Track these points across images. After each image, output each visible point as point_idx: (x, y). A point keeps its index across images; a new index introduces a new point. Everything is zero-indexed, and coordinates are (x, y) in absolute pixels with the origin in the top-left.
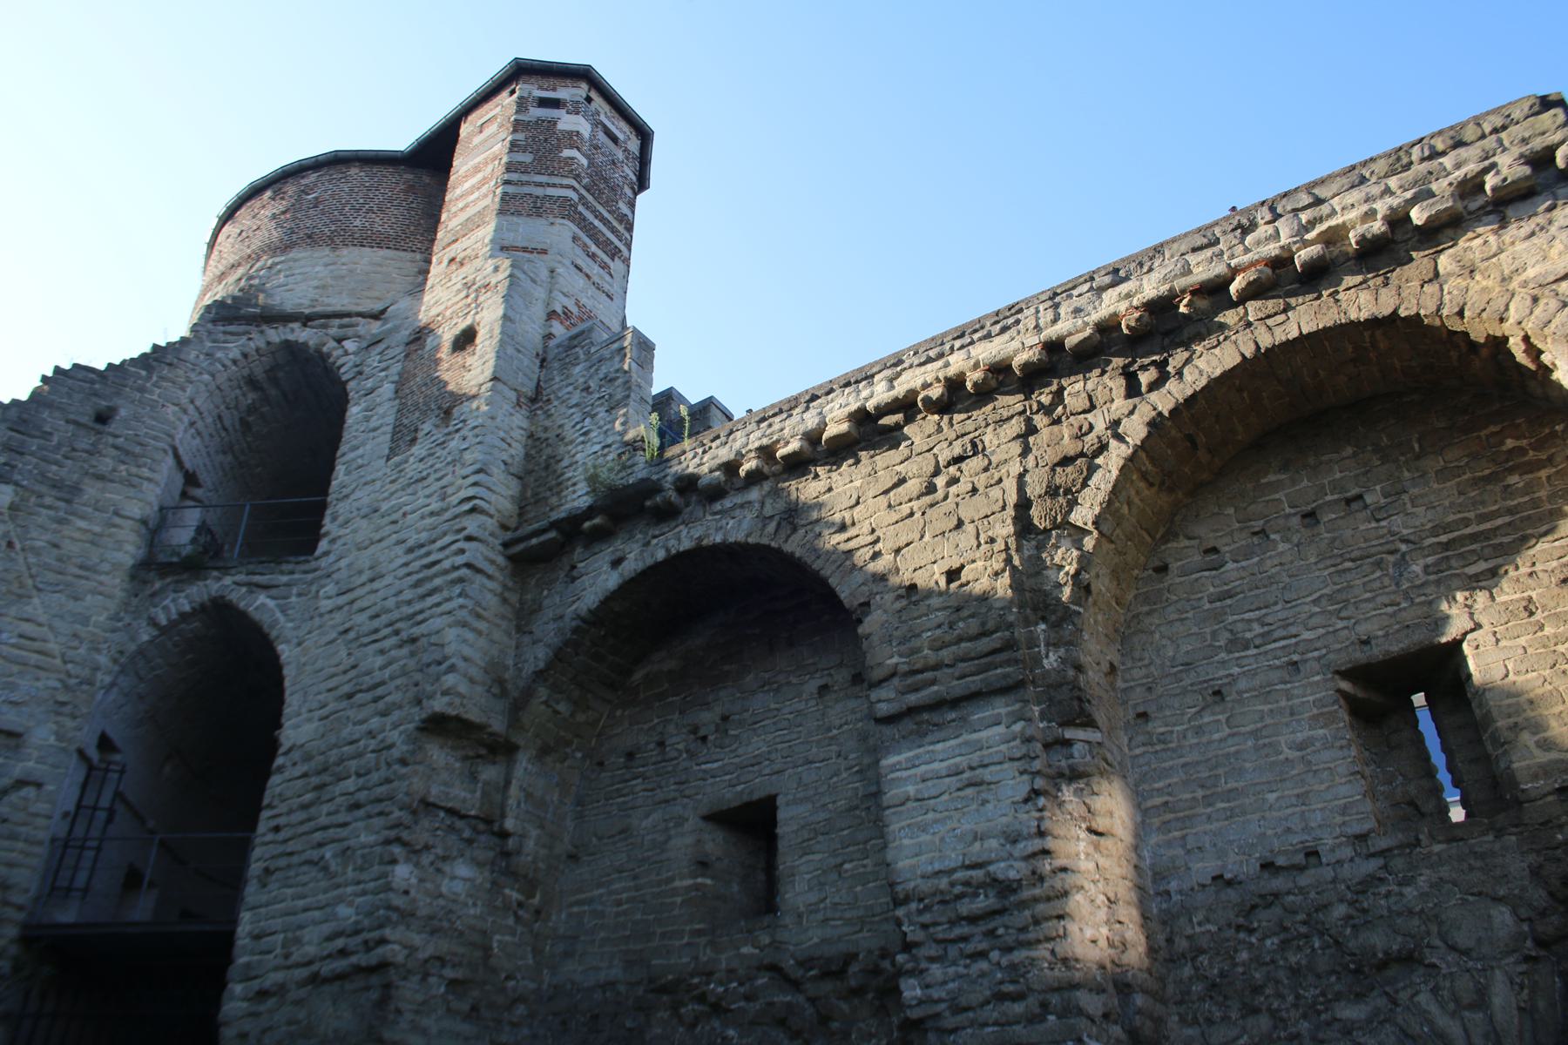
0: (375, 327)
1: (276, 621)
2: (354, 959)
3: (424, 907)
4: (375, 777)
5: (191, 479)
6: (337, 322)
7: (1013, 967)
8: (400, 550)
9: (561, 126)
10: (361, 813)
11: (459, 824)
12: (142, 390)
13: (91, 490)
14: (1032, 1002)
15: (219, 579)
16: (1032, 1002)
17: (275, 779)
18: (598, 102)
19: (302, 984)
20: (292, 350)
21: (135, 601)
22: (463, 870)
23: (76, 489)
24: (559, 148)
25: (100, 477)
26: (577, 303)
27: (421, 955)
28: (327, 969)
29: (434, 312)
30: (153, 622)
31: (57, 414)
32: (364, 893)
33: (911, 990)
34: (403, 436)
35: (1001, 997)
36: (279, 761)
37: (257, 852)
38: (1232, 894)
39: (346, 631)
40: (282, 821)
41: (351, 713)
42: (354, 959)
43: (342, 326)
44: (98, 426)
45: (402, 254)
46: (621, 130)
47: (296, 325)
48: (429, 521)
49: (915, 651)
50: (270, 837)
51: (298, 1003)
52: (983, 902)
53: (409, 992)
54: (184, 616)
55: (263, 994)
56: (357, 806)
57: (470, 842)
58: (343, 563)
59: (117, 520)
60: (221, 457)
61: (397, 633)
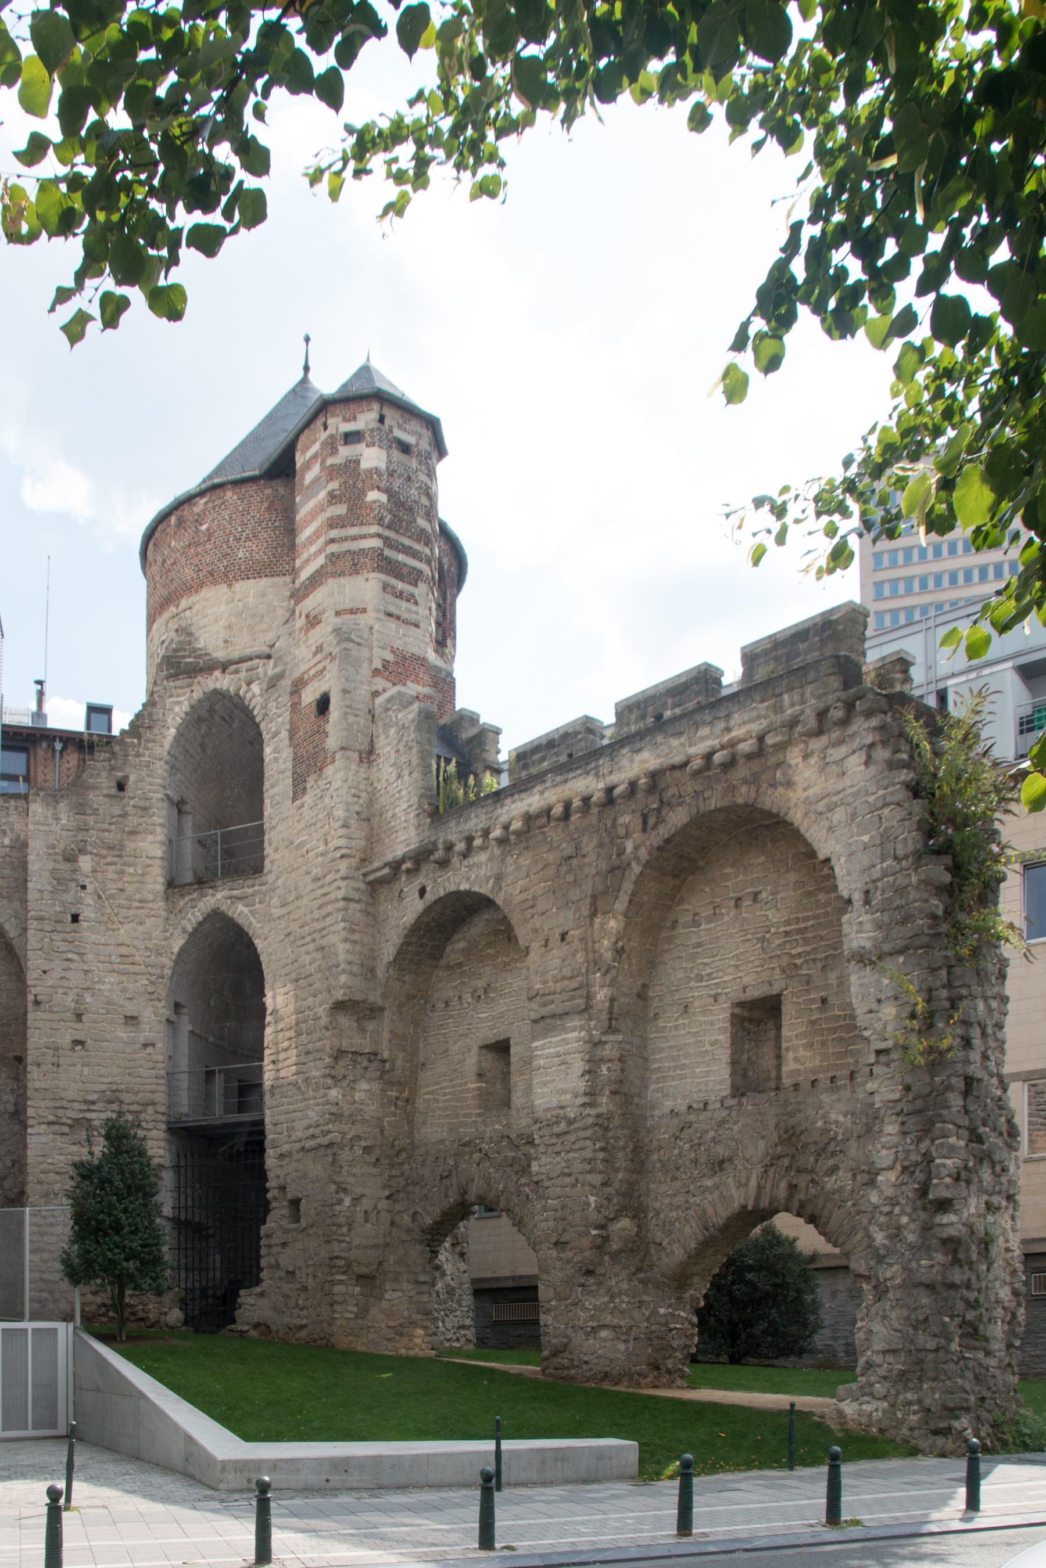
0: (271, 669)
1: (251, 923)
2: (318, 1140)
3: (347, 1110)
4: (315, 1036)
6: (244, 666)
7: (568, 1161)
9: (365, 465)
10: (311, 1057)
11: (359, 1059)
15: (213, 895)
17: (268, 1031)
19: (298, 1152)
20: (218, 695)
21: (172, 917)
22: (364, 1085)
24: (363, 493)
26: (393, 652)
27: (348, 1136)
29: (303, 668)
30: (184, 931)
39: (288, 935)
42: (318, 1140)
43: (247, 671)
45: (277, 580)
47: (217, 673)
48: (320, 859)
49: (546, 982)
50: (271, 1067)
51: (298, 1161)
52: (563, 1126)
53: (345, 1155)
54: (200, 924)
55: (282, 1156)
56: (308, 1053)
57: (366, 1068)
58: (280, 882)
61: (314, 940)
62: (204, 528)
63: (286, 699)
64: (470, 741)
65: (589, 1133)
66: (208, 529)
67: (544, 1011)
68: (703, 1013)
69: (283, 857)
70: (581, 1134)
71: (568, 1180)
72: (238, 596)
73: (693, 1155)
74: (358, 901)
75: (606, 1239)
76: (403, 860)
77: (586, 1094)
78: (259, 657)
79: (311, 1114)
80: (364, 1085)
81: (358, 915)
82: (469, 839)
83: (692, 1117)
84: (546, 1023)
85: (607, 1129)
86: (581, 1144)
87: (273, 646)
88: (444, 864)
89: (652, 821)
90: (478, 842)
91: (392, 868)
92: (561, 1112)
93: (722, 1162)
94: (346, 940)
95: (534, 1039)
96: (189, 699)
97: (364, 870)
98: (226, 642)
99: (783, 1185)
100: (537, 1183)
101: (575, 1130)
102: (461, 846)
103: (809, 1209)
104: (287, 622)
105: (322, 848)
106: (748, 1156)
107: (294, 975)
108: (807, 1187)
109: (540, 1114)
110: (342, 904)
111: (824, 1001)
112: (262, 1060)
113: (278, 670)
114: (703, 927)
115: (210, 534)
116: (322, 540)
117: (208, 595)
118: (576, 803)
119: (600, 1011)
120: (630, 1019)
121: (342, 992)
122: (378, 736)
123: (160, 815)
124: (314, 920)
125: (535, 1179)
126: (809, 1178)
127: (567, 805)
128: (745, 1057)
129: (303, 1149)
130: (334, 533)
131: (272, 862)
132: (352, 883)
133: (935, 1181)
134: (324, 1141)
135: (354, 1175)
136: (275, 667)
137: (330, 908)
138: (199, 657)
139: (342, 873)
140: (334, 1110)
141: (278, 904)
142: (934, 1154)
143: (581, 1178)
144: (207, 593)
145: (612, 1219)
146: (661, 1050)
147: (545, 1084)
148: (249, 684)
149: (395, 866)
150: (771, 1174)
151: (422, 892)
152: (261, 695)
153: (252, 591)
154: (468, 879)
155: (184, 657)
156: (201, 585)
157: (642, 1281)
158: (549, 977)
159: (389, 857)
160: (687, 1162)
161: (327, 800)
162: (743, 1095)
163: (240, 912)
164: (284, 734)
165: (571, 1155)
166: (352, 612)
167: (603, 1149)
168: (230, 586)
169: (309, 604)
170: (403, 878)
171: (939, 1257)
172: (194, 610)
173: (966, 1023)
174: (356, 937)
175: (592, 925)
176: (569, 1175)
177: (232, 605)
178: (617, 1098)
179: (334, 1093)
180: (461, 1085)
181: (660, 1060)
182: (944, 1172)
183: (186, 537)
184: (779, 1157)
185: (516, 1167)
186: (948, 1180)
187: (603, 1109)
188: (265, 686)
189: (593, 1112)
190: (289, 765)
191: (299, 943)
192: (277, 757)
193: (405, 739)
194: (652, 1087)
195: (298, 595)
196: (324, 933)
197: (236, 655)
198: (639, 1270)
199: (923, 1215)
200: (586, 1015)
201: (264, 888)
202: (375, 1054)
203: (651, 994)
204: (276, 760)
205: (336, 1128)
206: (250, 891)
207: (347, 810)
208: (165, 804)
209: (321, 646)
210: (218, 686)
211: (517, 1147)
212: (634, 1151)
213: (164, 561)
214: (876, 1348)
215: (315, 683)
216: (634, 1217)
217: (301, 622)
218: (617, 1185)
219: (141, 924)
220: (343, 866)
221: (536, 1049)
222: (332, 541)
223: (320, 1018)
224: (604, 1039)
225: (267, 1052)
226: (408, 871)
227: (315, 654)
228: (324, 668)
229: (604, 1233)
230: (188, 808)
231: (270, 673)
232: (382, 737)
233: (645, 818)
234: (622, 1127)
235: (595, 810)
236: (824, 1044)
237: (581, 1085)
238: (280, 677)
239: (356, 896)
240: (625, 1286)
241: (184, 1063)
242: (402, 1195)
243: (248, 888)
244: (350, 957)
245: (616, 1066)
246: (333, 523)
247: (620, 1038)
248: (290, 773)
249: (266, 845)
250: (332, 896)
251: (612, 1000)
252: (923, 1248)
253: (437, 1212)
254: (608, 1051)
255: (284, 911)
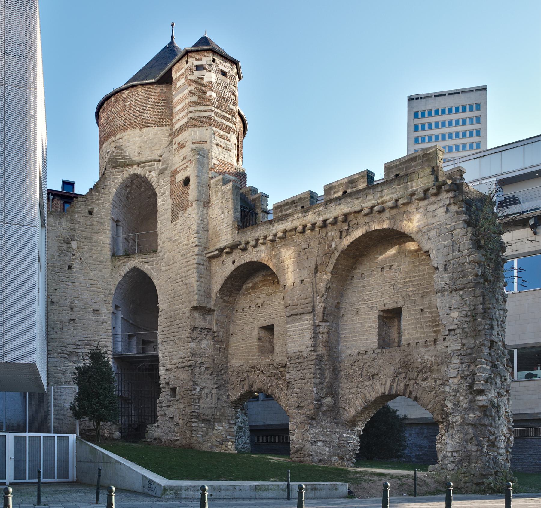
0: (160, 166)
1: (151, 273)
2: (185, 364)
4: (183, 321)
5: (117, 222)
7: (304, 373)
8: (180, 255)
10: (181, 329)
11: (203, 331)
12: (98, 200)
13: (95, 238)
14: (306, 381)
15: (134, 261)
16: (306, 381)
17: (160, 318)
18: (218, 60)
20: (136, 176)
21: (114, 269)
23: (91, 238)
25: (96, 233)
26: (218, 160)
28: (180, 365)
29: (177, 166)
30: (120, 275)
31: (79, 215)
32: (184, 349)
33: (288, 376)
34: (175, 216)
35: (302, 379)
36: (160, 313)
37: (159, 337)
38: (352, 358)
40: (163, 329)
41: (175, 302)
42: (185, 364)
44: (91, 216)
45: (163, 128)
46: (227, 67)
47: (135, 167)
48: (185, 247)
49: (293, 300)
50: (162, 333)
51: (174, 372)
52: (301, 359)
53: (197, 370)
54: (128, 272)
57: (206, 335)
58: (165, 256)
59: (104, 245)
60: (123, 210)
62: (128, 104)
63: (168, 179)
64: (254, 200)
65: (313, 362)
66: (130, 104)
67: (292, 312)
68: (365, 314)
69: (167, 246)
70: (309, 363)
71: (303, 381)
72: (145, 134)
73: (360, 372)
74: (203, 265)
75: (321, 405)
76: (225, 248)
77: (312, 346)
78: (154, 161)
79: (181, 353)
80: (205, 342)
81: (203, 270)
82: (257, 240)
83: (360, 357)
84: (293, 316)
85: (321, 361)
86: (310, 366)
87: (161, 156)
88: (244, 250)
89: (344, 234)
90: (261, 241)
91: (219, 251)
92: (301, 353)
93: (373, 375)
94: (198, 281)
95: (287, 324)
96: (122, 177)
97: (206, 252)
98: (139, 153)
99: (402, 385)
100: (289, 382)
101: (307, 361)
102: (253, 243)
103: (414, 394)
104: (168, 146)
105: (186, 242)
106: (386, 373)
107: (172, 295)
108: (413, 386)
109: (290, 355)
110: (196, 265)
111: (422, 310)
112: (157, 330)
113: (164, 166)
114: (365, 279)
115: (131, 106)
116: (186, 111)
117: (130, 133)
118: (309, 226)
119: (319, 313)
120: (332, 315)
121: (196, 302)
122: (213, 196)
123: (109, 226)
124: (182, 272)
125: (288, 381)
126: (414, 381)
127: (305, 227)
128: (384, 333)
129: (177, 367)
130: (191, 109)
131: (161, 248)
132: (200, 257)
133: (477, 382)
134: (189, 364)
135: (201, 378)
136: (162, 165)
137: (190, 267)
138: (126, 159)
139: (196, 253)
140: (192, 351)
141: (165, 265)
142: (477, 371)
143: (310, 380)
144: (130, 132)
145: (323, 398)
146: (345, 329)
147: (293, 342)
148: (150, 172)
149: (221, 250)
150: (397, 379)
151: (234, 262)
152: (156, 177)
153: (150, 132)
154: (256, 257)
155: (120, 159)
156: (127, 128)
157: (336, 423)
158: (295, 298)
159: (218, 247)
160: (357, 375)
161: (189, 222)
162: (383, 348)
163: (146, 268)
164: (167, 194)
165: (305, 371)
166: (200, 143)
167: (319, 369)
168: (141, 129)
169: (179, 138)
170: (224, 256)
171: (478, 413)
172: (124, 139)
173: (492, 319)
174: (202, 280)
175: (315, 277)
176: (304, 379)
177: (141, 138)
178: (326, 348)
179: (192, 344)
180: (250, 343)
181: (345, 334)
182: (481, 379)
183: (120, 107)
184: (400, 373)
185: (276, 377)
186: (482, 382)
187: (320, 353)
188: (157, 173)
189: (316, 354)
190: (170, 207)
191: (175, 282)
192: (164, 204)
193: (225, 197)
194: (341, 344)
195: (174, 135)
196: (187, 278)
197: (144, 159)
198: (335, 418)
199: (470, 396)
200: (312, 314)
201: (157, 258)
202: (211, 329)
203: (341, 307)
204: (163, 204)
205: (193, 359)
206: (151, 259)
207: (198, 226)
208: (111, 221)
209: (186, 157)
210: (136, 172)
211: (277, 368)
212: (333, 370)
213: (108, 117)
214: (448, 450)
215: (183, 172)
216: (333, 397)
217: (175, 146)
218: (326, 384)
219: (100, 271)
220: (196, 249)
221: (289, 328)
222: (191, 112)
223: (185, 313)
224: (320, 324)
225: (159, 327)
226: (227, 253)
227: (182, 160)
228: (187, 166)
229: (320, 403)
230: (120, 224)
231: (160, 167)
232: (214, 196)
233: (341, 233)
234: (328, 360)
235: (317, 229)
236: (422, 327)
237: (310, 343)
238: (165, 169)
239: (202, 262)
240: (329, 425)
241: (119, 331)
242: (222, 387)
243: (151, 258)
244: (200, 288)
245: (325, 335)
246: (191, 104)
247: (328, 324)
248: (171, 210)
249: (159, 240)
250: (191, 262)
251: (324, 308)
252: (471, 409)
253: (239, 395)
254: (322, 329)
255: (167, 268)
